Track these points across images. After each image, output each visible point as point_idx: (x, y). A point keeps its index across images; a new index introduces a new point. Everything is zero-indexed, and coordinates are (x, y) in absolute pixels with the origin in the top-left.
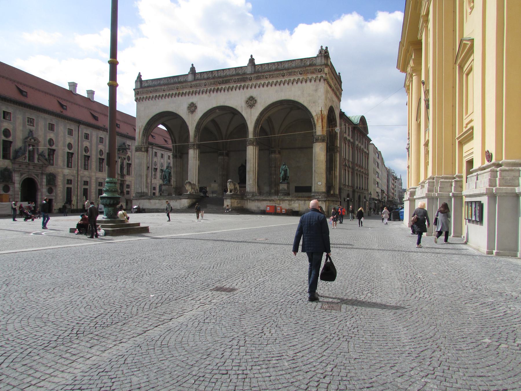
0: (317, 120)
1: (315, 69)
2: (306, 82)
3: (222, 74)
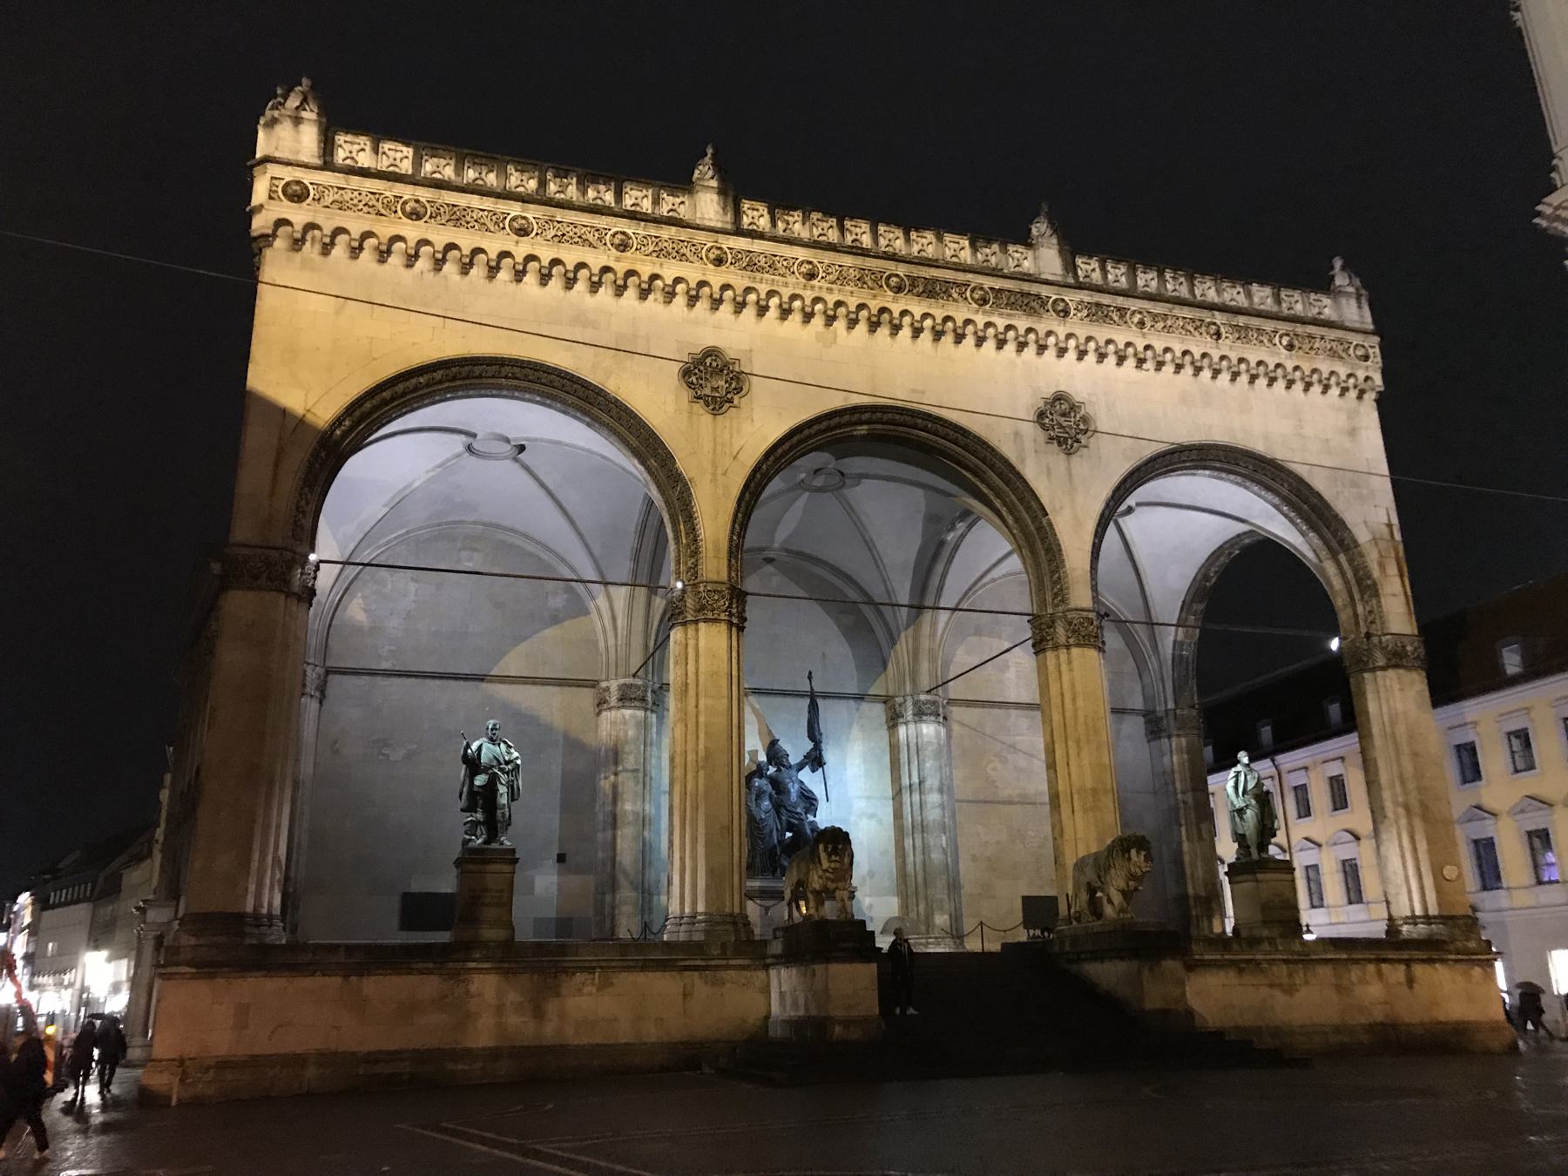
0: (1382, 566)
1: (1340, 341)
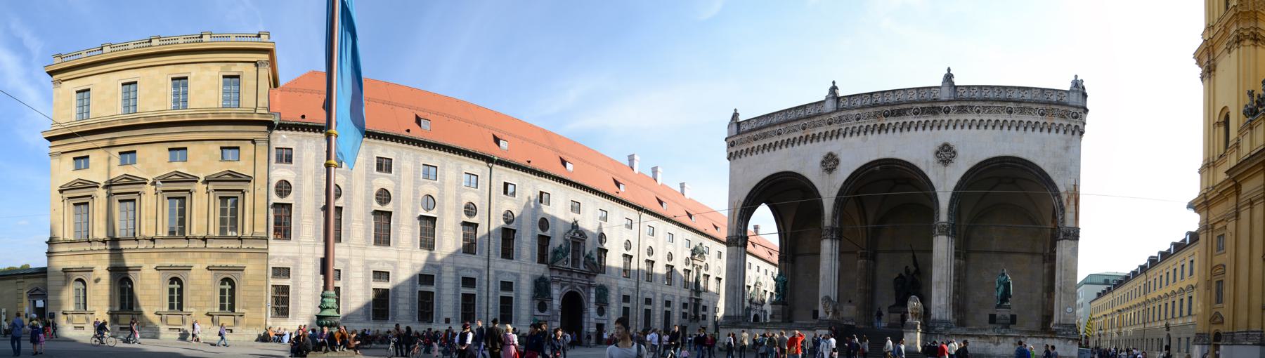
2: (1049, 130)
3: (892, 99)
